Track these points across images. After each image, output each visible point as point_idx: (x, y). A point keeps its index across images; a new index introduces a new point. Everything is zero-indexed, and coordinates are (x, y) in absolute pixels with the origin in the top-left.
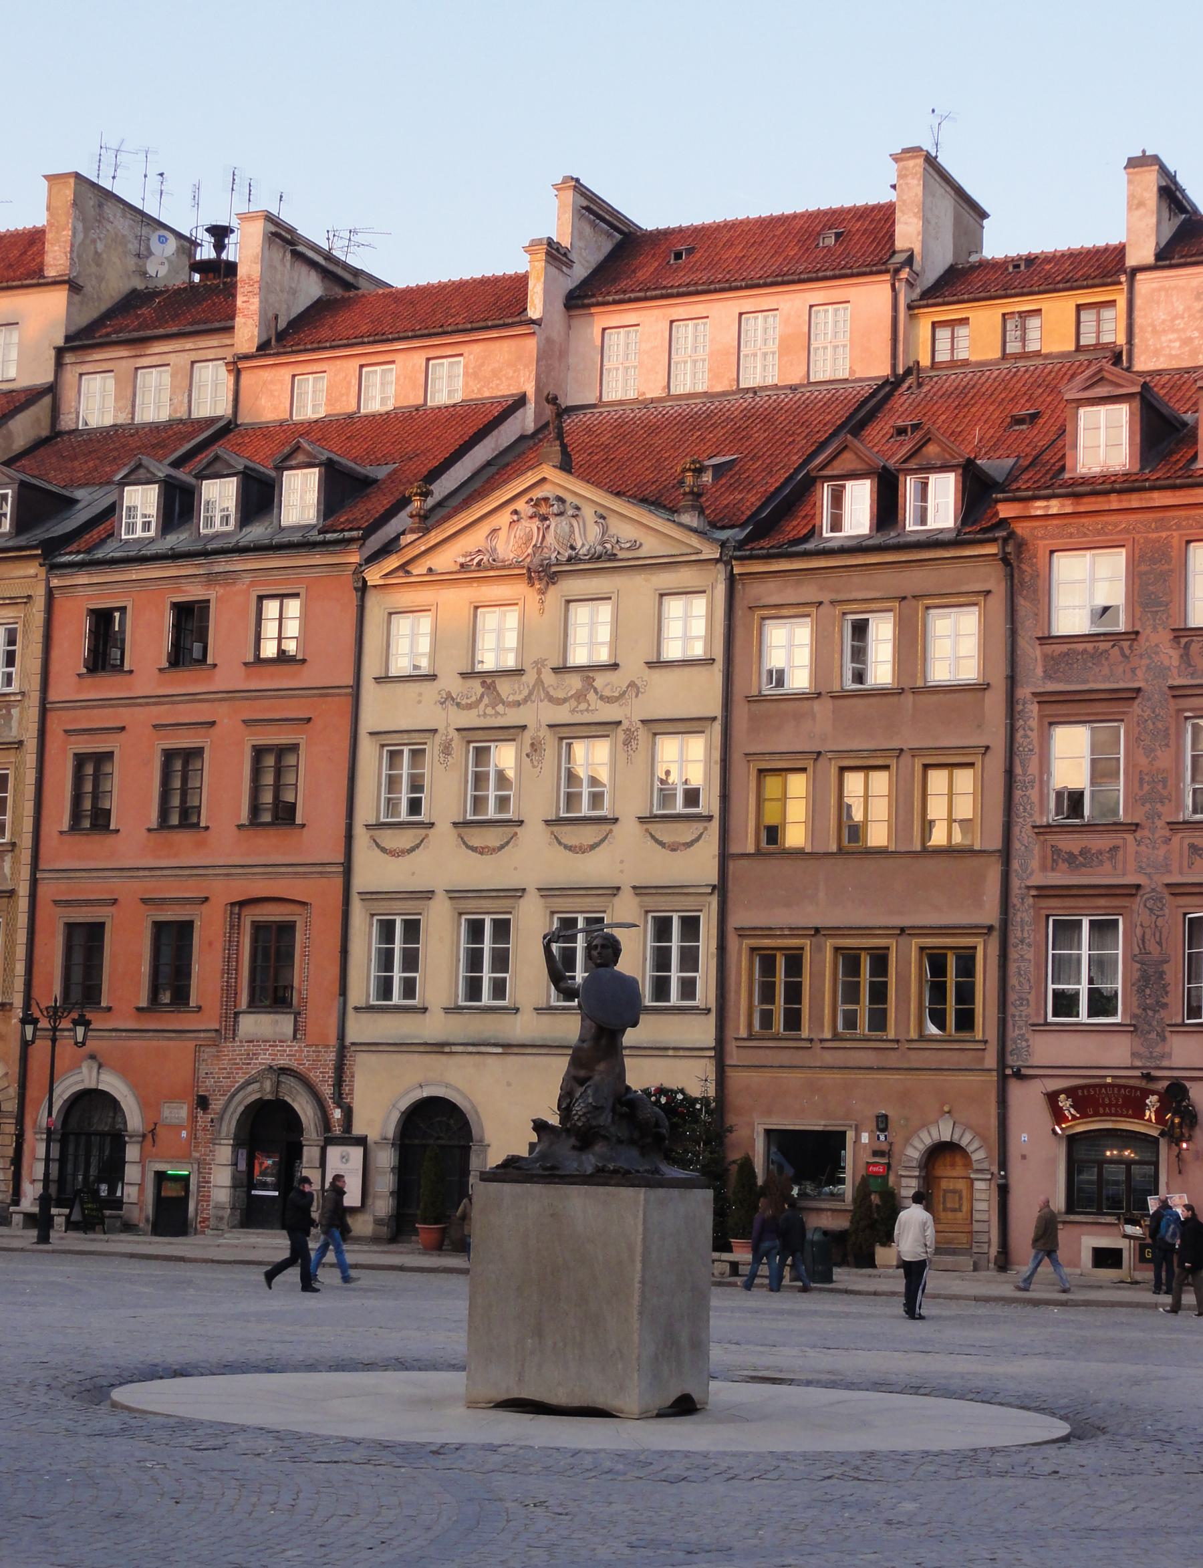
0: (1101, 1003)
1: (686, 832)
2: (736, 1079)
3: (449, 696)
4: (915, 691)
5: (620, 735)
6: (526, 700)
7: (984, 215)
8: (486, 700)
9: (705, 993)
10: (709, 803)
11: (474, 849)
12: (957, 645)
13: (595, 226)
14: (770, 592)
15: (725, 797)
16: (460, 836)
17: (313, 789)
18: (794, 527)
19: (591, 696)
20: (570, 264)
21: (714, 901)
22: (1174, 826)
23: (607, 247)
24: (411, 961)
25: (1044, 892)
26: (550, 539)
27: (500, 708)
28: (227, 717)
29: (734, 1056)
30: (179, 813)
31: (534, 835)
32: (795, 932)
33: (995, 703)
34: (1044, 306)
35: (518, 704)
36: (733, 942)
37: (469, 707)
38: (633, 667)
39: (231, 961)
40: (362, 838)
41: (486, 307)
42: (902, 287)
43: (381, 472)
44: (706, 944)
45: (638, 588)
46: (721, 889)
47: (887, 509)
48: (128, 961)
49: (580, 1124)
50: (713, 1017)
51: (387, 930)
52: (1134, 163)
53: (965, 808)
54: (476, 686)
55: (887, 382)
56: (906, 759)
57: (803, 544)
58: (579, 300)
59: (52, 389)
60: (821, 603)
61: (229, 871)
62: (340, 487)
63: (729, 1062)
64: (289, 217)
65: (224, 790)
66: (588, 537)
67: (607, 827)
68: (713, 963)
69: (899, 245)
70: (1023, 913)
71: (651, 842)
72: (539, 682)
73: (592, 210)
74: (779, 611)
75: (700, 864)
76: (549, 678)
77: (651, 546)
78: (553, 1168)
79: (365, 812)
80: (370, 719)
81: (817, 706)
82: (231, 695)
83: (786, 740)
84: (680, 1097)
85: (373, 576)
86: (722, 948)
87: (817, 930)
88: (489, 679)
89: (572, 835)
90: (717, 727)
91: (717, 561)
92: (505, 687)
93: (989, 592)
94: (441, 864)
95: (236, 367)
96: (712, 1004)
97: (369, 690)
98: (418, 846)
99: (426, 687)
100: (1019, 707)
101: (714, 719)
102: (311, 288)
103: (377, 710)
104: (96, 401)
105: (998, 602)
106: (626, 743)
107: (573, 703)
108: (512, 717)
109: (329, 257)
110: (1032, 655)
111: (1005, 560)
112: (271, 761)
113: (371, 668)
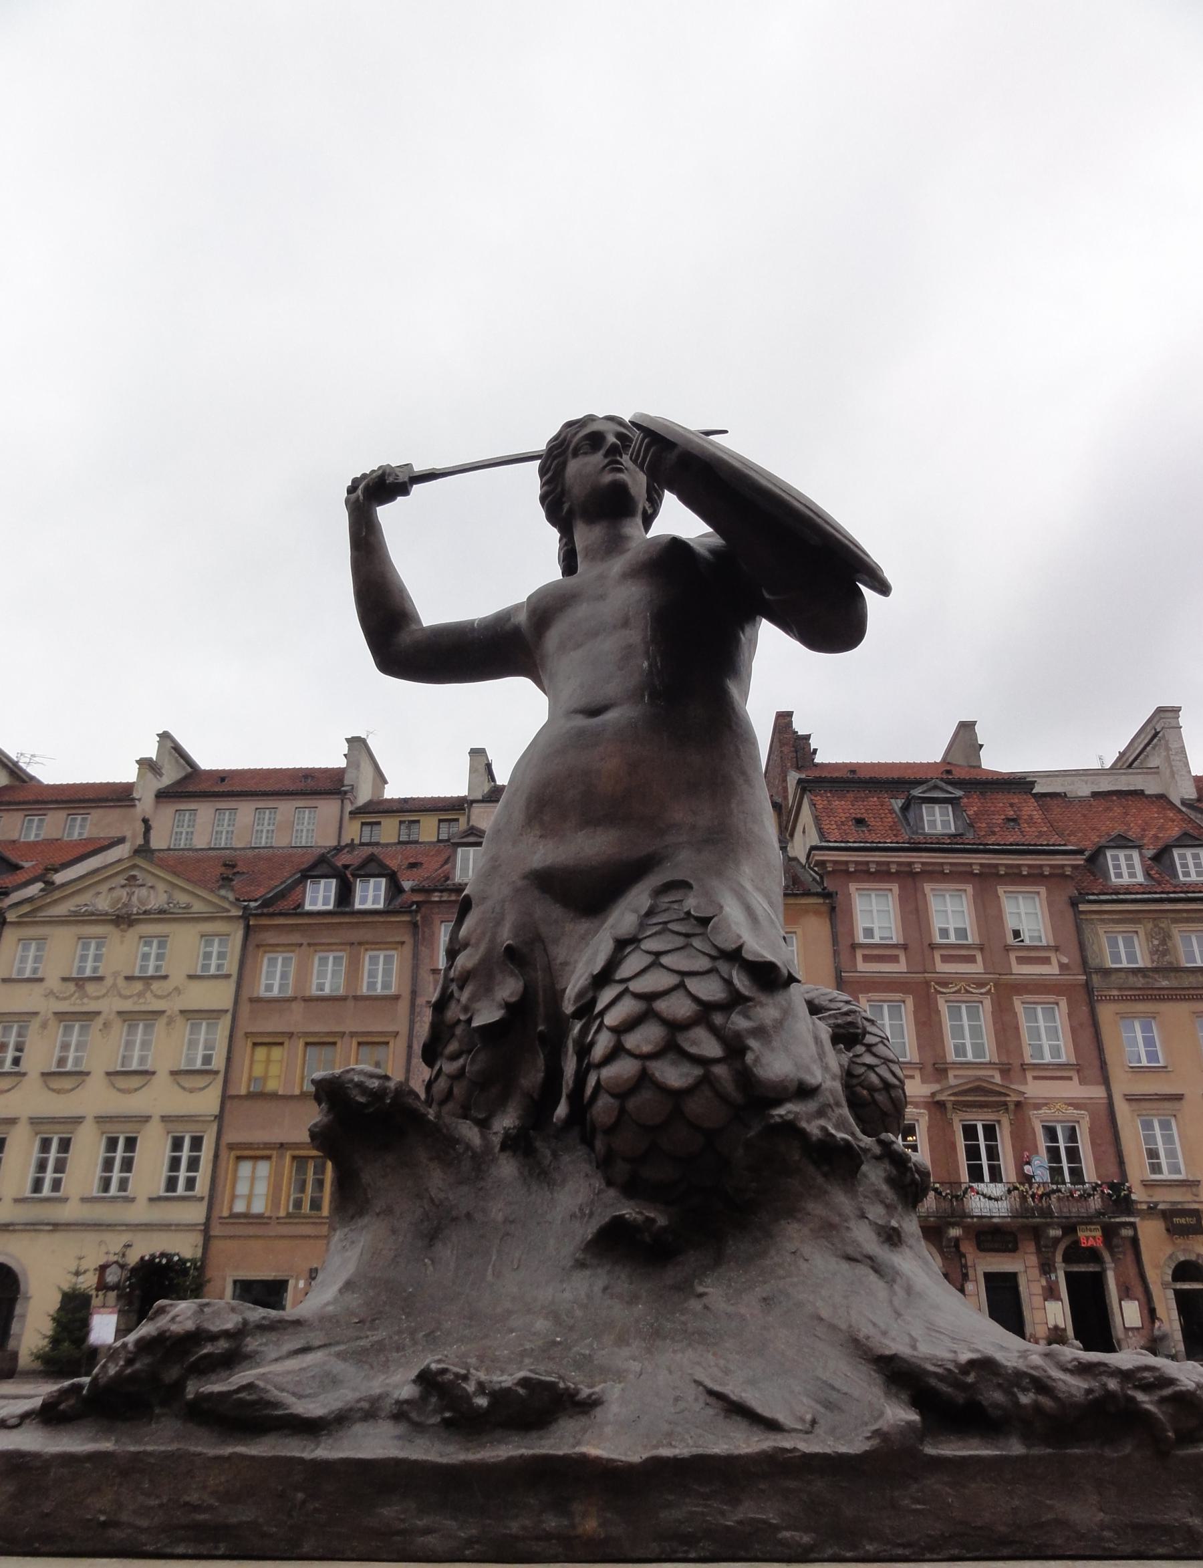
1: (200, 1081)
2: (216, 1245)
3: (52, 993)
4: (356, 998)
5: (163, 1020)
6: (104, 996)
7: (386, 782)
8: (77, 995)
9: (202, 1187)
10: (218, 1063)
11: (53, 1090)
13: (177, 761)
14: (271, 938)
15: (229, 1059)
16: (45, 1082)
18: (284, 905)
19: (148, 995)
20: (161, 775)
21: (214, 1127)
23: (182, 774)
26: (134, 899)
27: (85, 1000)
29: (216, 1230)
31: (96, 1082)
32: (267, 1146)
33: (403, 1007)
34: (422, 819)
35: (98, 998)
36: (224, 1153)
37: (65, 999)
42: (347, 802)
43: (26, 865)
44: (206, 1154)
46: (220, 1118)
47: (345, 895)
50: (205, 1203)
54: (72, 987)
55: (335, 848)
56: (346, 1039)
58: (163, 796)
60: (301, 945)
63: (212, 1233)
66: (157, 900)
67: (148, 1077)
68: (210, 1166)
69: (346, 782)
71: (176, 1087)
72: (114, 985)
74: (274, 947)
75: (207, 1101)
76: (121, 982)
77: (198, 907)
81: (294, 1005)
83: (272, 1024)
84: (176, 1258)
85: (11, 917)
86: (216, 1156)
87: (282, 1145)
88: (79, 982)
89: (122, 1083)
90: (229, 1016)
91: (240, 917)
92: (91, 988)
93: (403, 943)
96: (206, 1193)
98: (13, 1088)
99: (36, 986)
100: (417, 1010)
101: (227, 1011)
105: (407, 950)
106: (168, 1024)
107: (135, 998)
108: (92, 1006)
109: (16, 764)
111: (415, 925)
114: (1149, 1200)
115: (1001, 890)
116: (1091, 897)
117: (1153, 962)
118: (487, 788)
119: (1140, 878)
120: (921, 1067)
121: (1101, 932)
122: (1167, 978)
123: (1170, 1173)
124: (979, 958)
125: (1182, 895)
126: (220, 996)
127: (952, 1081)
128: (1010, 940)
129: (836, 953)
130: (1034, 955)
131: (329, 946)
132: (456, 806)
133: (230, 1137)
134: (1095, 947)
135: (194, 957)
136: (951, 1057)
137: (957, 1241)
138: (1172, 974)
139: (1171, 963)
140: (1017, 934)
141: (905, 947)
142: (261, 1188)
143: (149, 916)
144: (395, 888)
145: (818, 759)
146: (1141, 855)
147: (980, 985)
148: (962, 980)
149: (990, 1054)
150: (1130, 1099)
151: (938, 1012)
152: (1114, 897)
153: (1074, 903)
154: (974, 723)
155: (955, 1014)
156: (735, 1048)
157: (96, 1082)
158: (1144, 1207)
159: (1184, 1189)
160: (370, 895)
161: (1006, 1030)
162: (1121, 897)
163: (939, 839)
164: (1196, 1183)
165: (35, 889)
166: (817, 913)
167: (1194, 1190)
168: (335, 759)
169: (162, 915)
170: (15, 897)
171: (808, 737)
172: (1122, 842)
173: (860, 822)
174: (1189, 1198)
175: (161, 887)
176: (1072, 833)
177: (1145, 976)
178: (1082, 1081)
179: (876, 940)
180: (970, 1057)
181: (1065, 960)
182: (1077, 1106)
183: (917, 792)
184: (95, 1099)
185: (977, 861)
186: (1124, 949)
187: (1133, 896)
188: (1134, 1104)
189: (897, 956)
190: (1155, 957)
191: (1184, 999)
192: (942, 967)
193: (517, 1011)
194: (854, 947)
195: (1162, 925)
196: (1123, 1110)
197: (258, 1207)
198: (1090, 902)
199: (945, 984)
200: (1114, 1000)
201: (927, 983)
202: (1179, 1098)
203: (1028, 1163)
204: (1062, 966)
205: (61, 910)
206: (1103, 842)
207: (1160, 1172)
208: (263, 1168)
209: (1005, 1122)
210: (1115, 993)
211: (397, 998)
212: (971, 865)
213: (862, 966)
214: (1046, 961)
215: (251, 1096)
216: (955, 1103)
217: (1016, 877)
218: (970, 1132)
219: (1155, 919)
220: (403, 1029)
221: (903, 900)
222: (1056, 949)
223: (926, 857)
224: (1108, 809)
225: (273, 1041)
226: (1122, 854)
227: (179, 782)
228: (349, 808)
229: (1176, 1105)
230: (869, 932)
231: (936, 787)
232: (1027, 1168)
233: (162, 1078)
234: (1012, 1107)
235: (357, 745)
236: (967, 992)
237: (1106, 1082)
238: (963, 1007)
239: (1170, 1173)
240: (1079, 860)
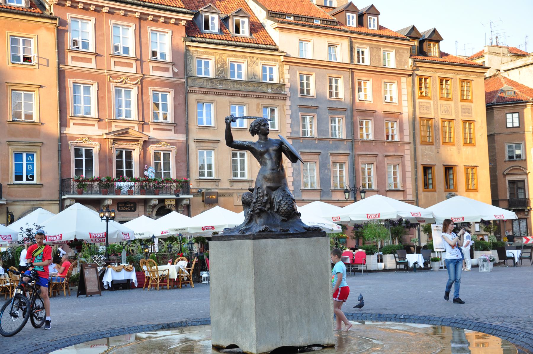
49: (289, 209)
78: (288, 230)
114: (197, 188)
116: (194, 39)
117: (216, 75)
122: (220, 84)
123: (208, 176)
125: (235, 43)
127: (114, 129)
134: (191, 65)
137: (108, 206)
138: (224, 83)
139: (224, 77)
140: (154, 54)
146: (219, 17)
148: (125, 76)
149: (134, 116)
151: (109, 92)
152: (204, 40)
156: (293, 206)
158: (194, 191)
159: (212, 183)
162: (208, 40)
166: (48, 29)
167: (217, 183)
174: (214, 187)
177: (211, 82)
178: (176, 132)
180: (123, 117)
181: (176, 70)
182: (172, 144)
187: (212, 41)
188: (197, 143)
189: (91, 59)
190: (217, 73)
192: (114, 68)
193: (267, 200)
195: (223, 57)
196: (192, 145)
198: (193, 41)
199: (116, 78)
203: (147, 170)
204: (174, 73)
207: (203, 175)
210: (197, 89)
212: (135, 12)
213: (70, 62)
216: (115, 140)
219: (220, 54)
222: (173, 64)
229: (215, 145)
234: (141, 142)
236: (126, 83)
237: (187, 131)
238: (123, 89)
239: (208, 176)
240: (190, 18)
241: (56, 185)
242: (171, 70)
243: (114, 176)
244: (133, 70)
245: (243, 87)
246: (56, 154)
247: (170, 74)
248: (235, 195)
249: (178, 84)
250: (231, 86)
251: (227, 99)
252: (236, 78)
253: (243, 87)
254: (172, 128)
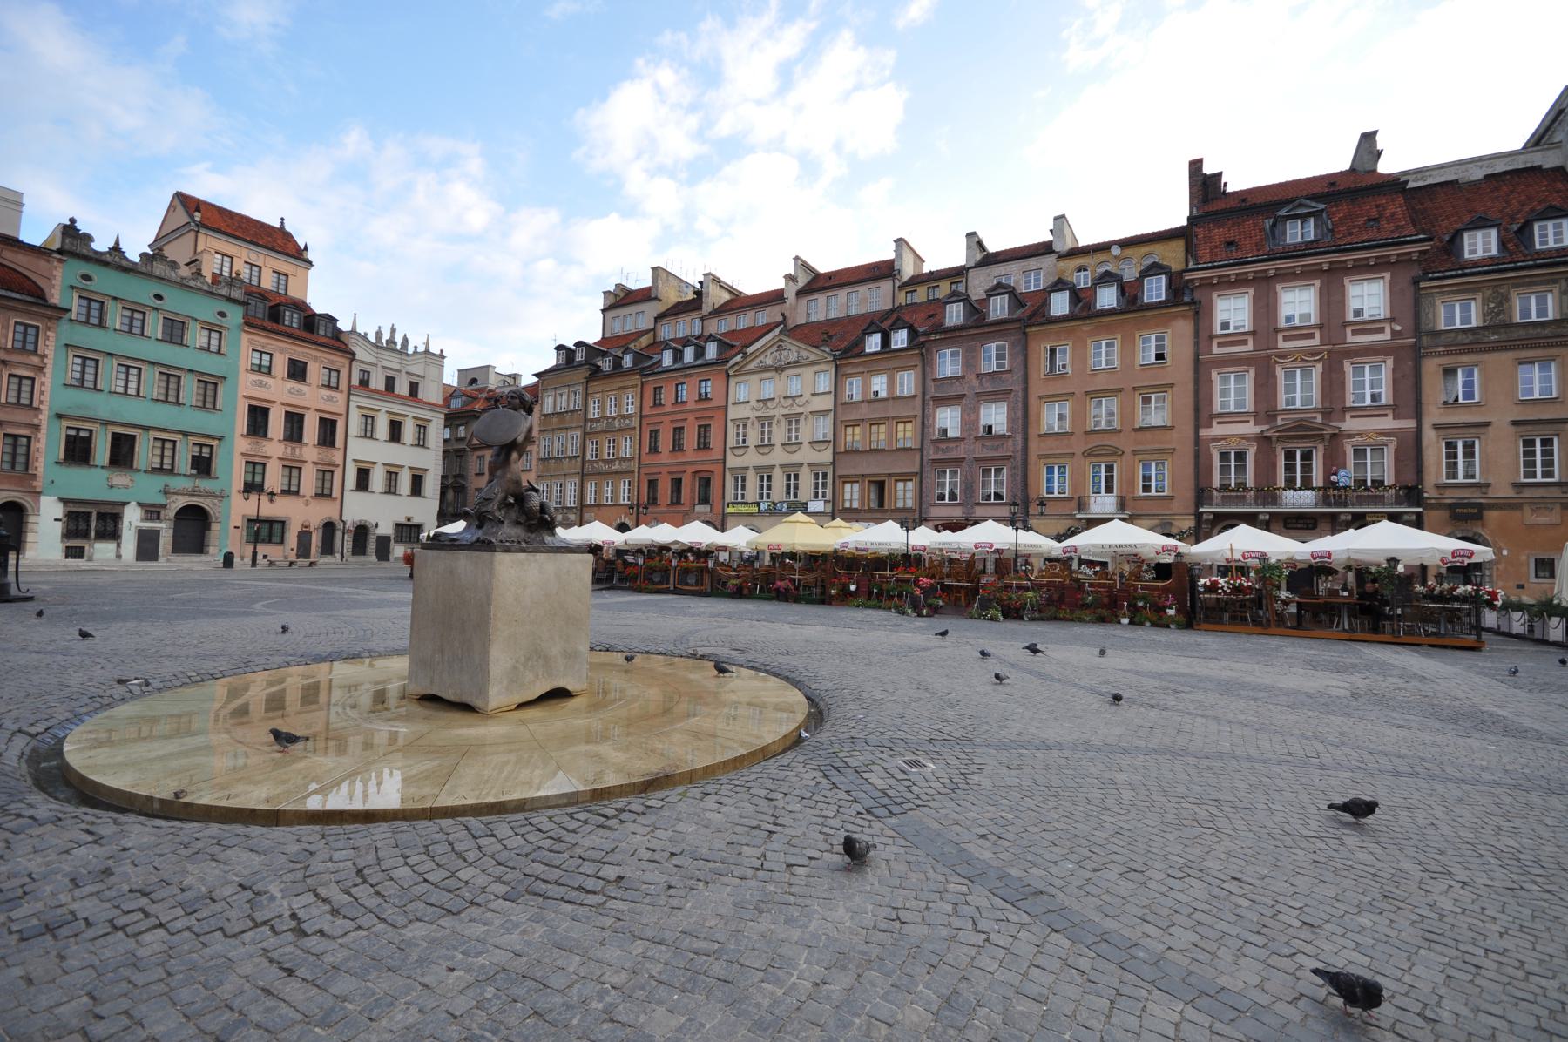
0: (953, 496)
1: (823, 446)
10: (830, 437)
12: (907, 382)
17: (715, 439)
18: (856, 350)
22: (976, 439)
24: (743, 488)
25: (934, 461)
28: (691, 418)
30: (678, 447)
31: (778, 449)
33: (918, 401)
38: (807, 396)
39: (692, 490)
40: (728, 452)
41: (776, 297)
45: (808, 372)
46: (833, 463)
47: (886, 342)
48: (665, 489)
51: (736, 479)
52: (969, 235)
53: (909, 435)
57: (862, 353)
58: (800, 293)
59: (653, 329)
61: (691, 463)
62: (724, 346)
64: (718, 275)
65: (690, 439)
66: (793, 357)
70: (927, 468)
73: (802, 264)
74: (851, 375)
75: (826, 456)
77: (812, 357)
79: (729, 445)
80: (731, 416)
82: (691, 411)
83: (853, 415)
88: (764, 401)
89: (789, 449)
94: (751, 459)
95: (702, 319)
97: (730, 407)
102: (727, 297)
103: (733, 413)
104: (666, 332)
105: (919, 369)
110: (931, 386)
112: (704, 430)
113: (731, 400)
115: (1346, 281)
118: (979, 256)
119: (1494, 252)
120: (1256, 414)
121: (1438, 302)
124: (1317, 335)
126: (827, 403)
128: (1350, 317)
129: (1197, 344)
130: (1373, 326)
131: (878, 372)
132: (957, 273)
133: (839, 472)
135: (814, 383)
136: (1282, 405)
141: (1253, 333)
142: (856, 496)
143: (789, 365)
144: (913, 334)
145: (1229, 189)
147: (1314, 354)
149: (1316, 400)
150: (1437, 427)
153: (1416, 282)
154: (1375, 133)
155: (1290, 376)
157: (778, 449)
160: (900, 339)
161: (1333, 384)
163: (1295, 247)
164: (1488, 485)
165: (739, 358)
166: (1184, 317)
168: (890, 255)
169: (797, 364)
170: (732, 362)
171: (1219, 175)
172: (1481, 224)
173: (1230, 244)
175: (794, 349)
176: (1448, 218)
179: (1232, 330)
181: (1398, 328)
183: (1282, 213)
184: (778, 457)
185: (1325, 260)
186: (1458, 313)
191: (1507, 349)
192: (1281, 344)
194: (1212, 337)
196: (1429, 435)
197: (856, 505)
199: (1284, 357)
200: (1439, 355)
201: (1269, 357)
202: (1487, 424)
204: (1393, 333)
205: (752, 366)
206: (1459, 226)
208: (856, 487)
209: (1321, 448)
211: (914, 397)
214: (1381, 330)
215: (846, 452)
217: (1364, 269)
218: (1290, 456)
220: (919, 413)
221: (1256, 301)
222: (1392, 320)
223: (1280, 264)
224: (1497, 189)
225: (854, 424)
226: (1479, 234)
227: (809, 283)
228: (898, 284)
230: (1225, 326)
231: (1300, 205)
232: (1333, 478)
233: (806, 445)
235: (900, 242)
237: (1418, 416)
241: (1188, 494)
242: (1388, 330)
243: (1281, 482)
244: (1316, 341)
245: (1547, 331)
246: (1192, 461)
247: (1387, 336)
248: (1527, 509)
249: (1402, 347)
250: (1522, 333)
251: (1508, 356)
252: (1534, 318)
253: (1547, 331)
254: (1390, 413)
